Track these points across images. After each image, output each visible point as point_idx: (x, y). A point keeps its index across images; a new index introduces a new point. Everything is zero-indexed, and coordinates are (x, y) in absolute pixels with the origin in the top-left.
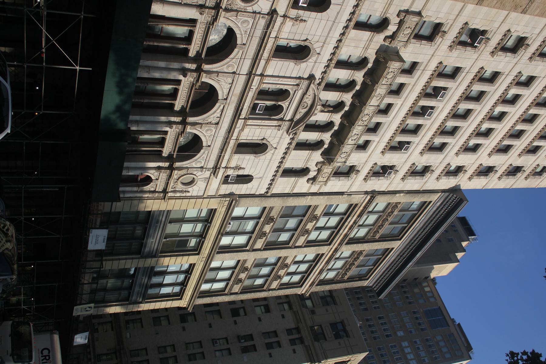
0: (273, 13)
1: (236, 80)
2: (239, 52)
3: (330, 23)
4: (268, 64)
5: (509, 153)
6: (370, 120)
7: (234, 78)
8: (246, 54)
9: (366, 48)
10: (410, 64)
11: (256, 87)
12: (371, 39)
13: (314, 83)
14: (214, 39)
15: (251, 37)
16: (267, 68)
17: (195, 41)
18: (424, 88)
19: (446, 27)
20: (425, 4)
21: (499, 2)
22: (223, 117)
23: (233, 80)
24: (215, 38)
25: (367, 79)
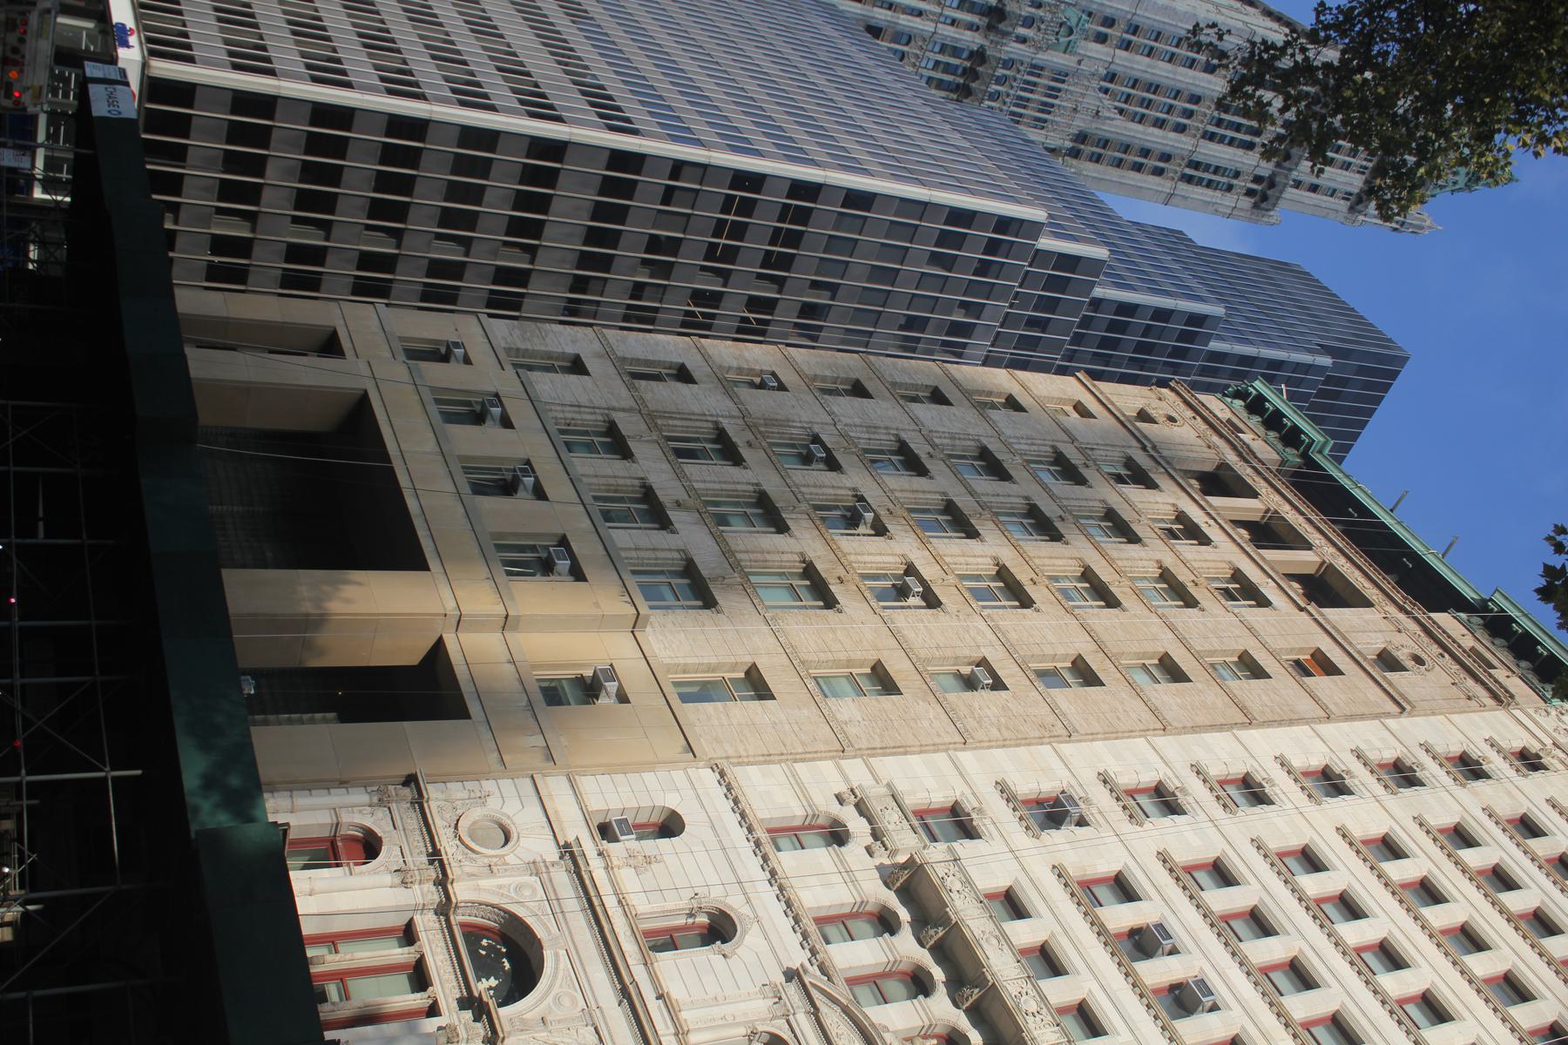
0: (568, 852)
1: (603, 1025)
2: (557, 955)
3: (718, 856)
4: (652, 964)
5: (1449, 893)
6: (1045, 1004)
7: (592, 1017)
8: (577, 952)
9: (852, 882)
10: (1082, 1029)
11: (672, 1030)
12: (841, 861)
13: (805, 971)
14: (490, 988)
15: (560, 915)
16: (658, 973)
17: (439, 975)
18: (1096, 929)
19: (968, 801)
20: (871, 772)
21: (1003, 730)
22: (606, 1033)
23: (596, 1029)
24: (494, 985)
25: (927, 932)
